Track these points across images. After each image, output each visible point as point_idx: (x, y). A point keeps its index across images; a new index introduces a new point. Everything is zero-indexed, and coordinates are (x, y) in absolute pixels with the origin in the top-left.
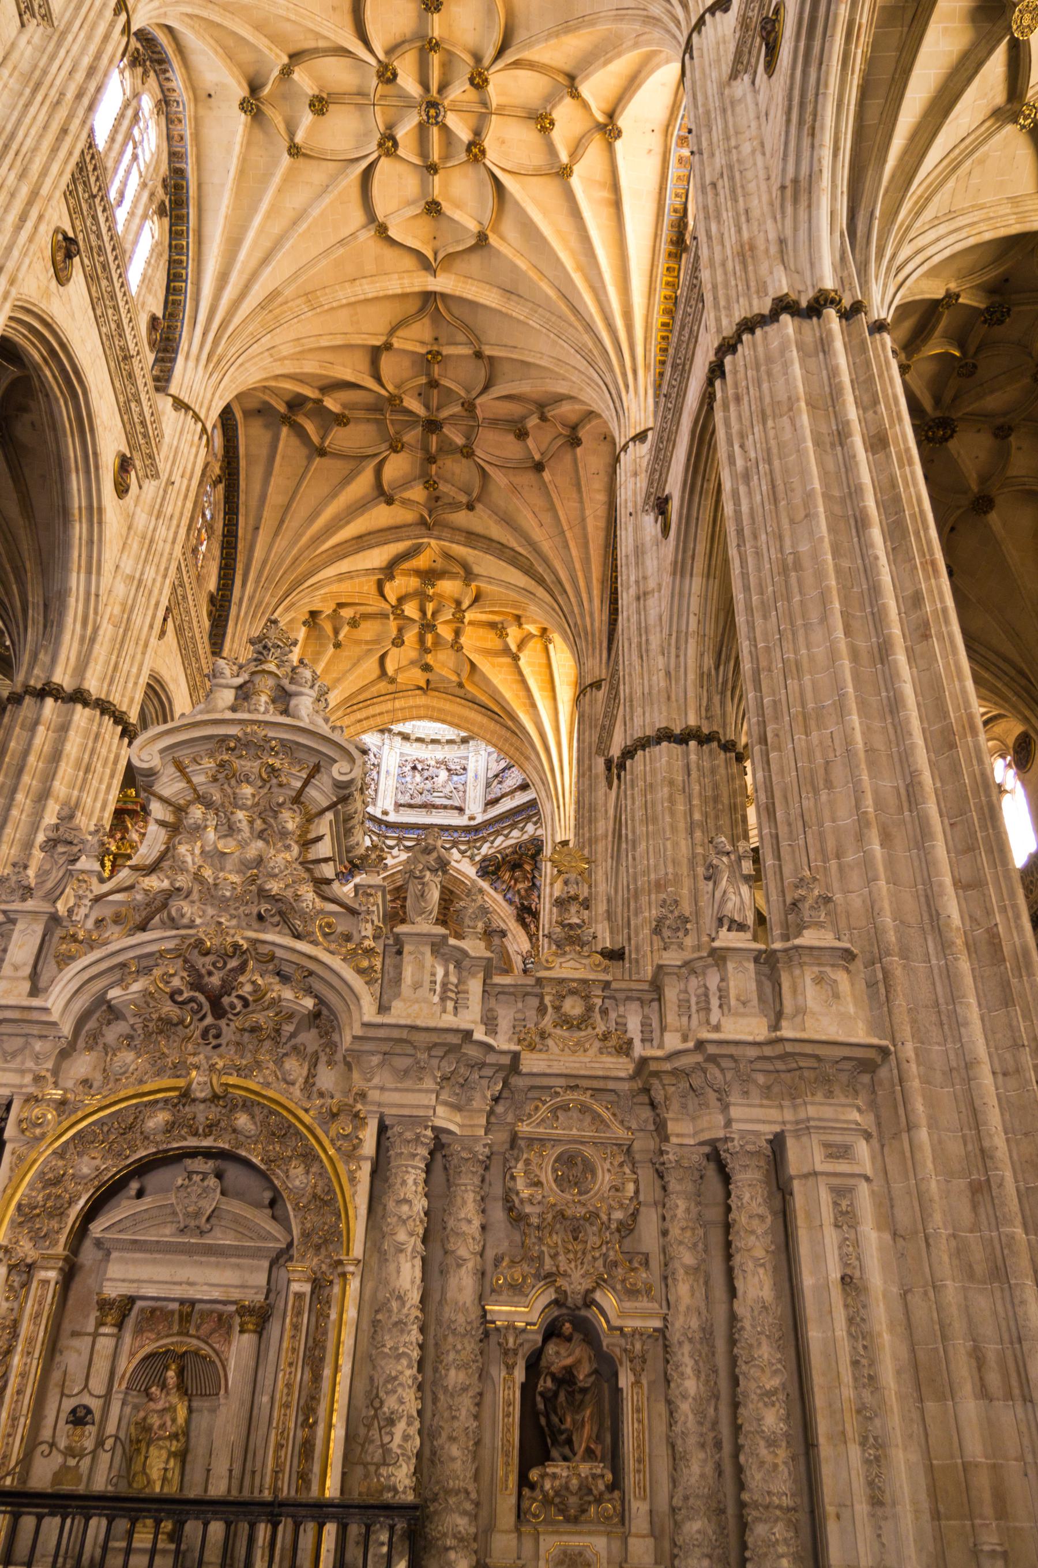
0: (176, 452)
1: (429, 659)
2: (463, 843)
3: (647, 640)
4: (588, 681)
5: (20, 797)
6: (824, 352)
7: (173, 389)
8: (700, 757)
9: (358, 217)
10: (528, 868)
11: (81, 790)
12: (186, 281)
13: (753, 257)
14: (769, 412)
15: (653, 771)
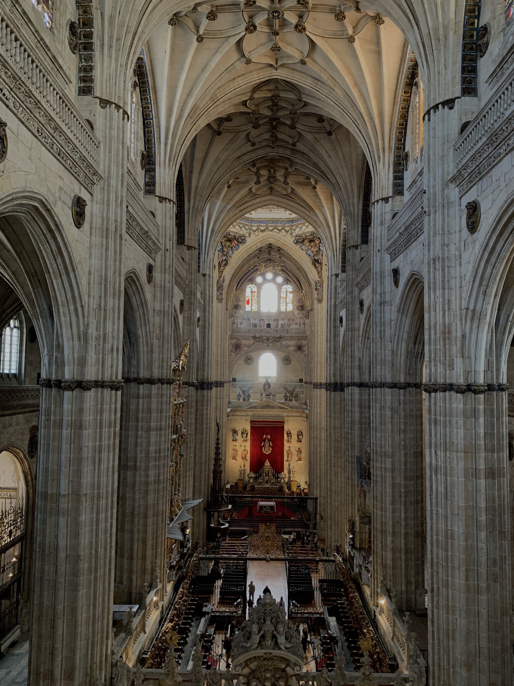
0: (165, 231)
1: (273, 185)
2: (287, 226)
3: (384, 330)
4: (352, 244)
5: (140, 433)
6: (475, 417)
7: (157, 194)
8: (405, 396)
9: (235, 56)
10: (317, 242)
11: (161, 421)
12: (152, 119)
13: (449, 339)
14: (448, 446)
15: (385, 400)
